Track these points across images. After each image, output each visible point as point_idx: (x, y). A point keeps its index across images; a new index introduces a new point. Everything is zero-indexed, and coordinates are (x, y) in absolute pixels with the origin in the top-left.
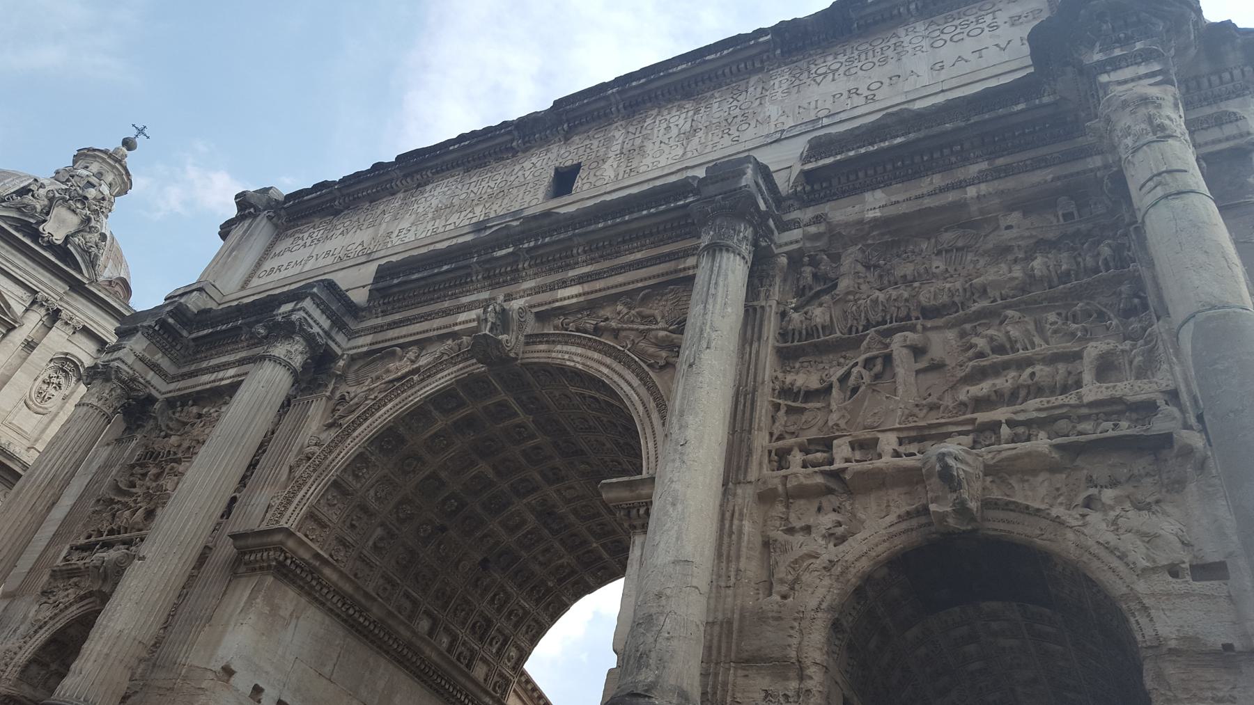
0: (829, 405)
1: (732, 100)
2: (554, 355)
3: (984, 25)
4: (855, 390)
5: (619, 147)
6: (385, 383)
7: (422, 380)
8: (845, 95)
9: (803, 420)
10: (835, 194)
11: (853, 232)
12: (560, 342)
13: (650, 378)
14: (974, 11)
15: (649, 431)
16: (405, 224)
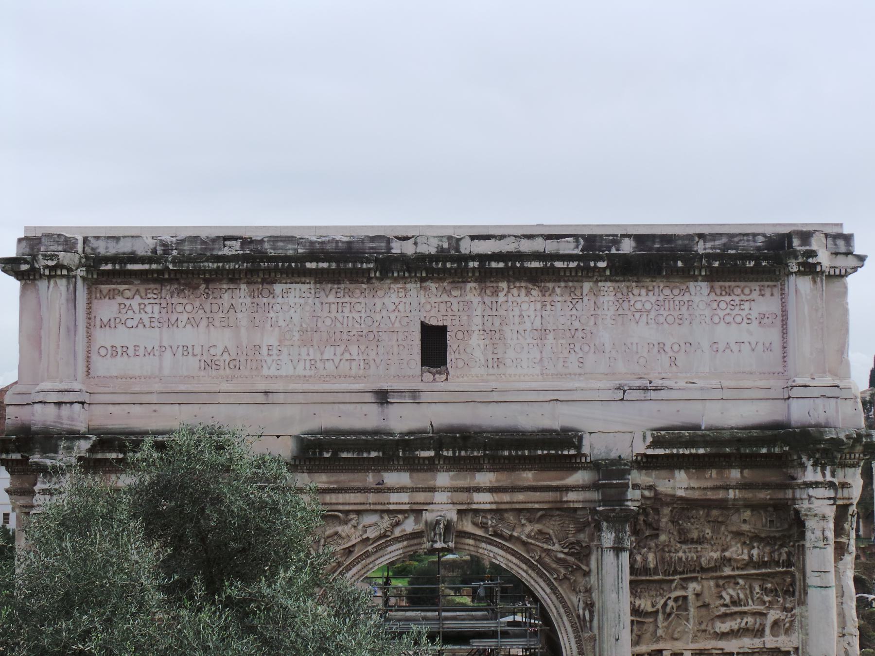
0: (656, 620)
1: (571, 306)
2: (481, 551)
3: (744, 313)
4: (670, 615)
5: (477, 320)
6: (343, 549)
7: (376, 552)
8: (656, 345)
9: (644, 629)
10: (659, 466)
11: (668, 500)
12: (483, 542)
13: (559, 591)
14: (738, 291)
15: (563, 628)
16: (271, 339)
